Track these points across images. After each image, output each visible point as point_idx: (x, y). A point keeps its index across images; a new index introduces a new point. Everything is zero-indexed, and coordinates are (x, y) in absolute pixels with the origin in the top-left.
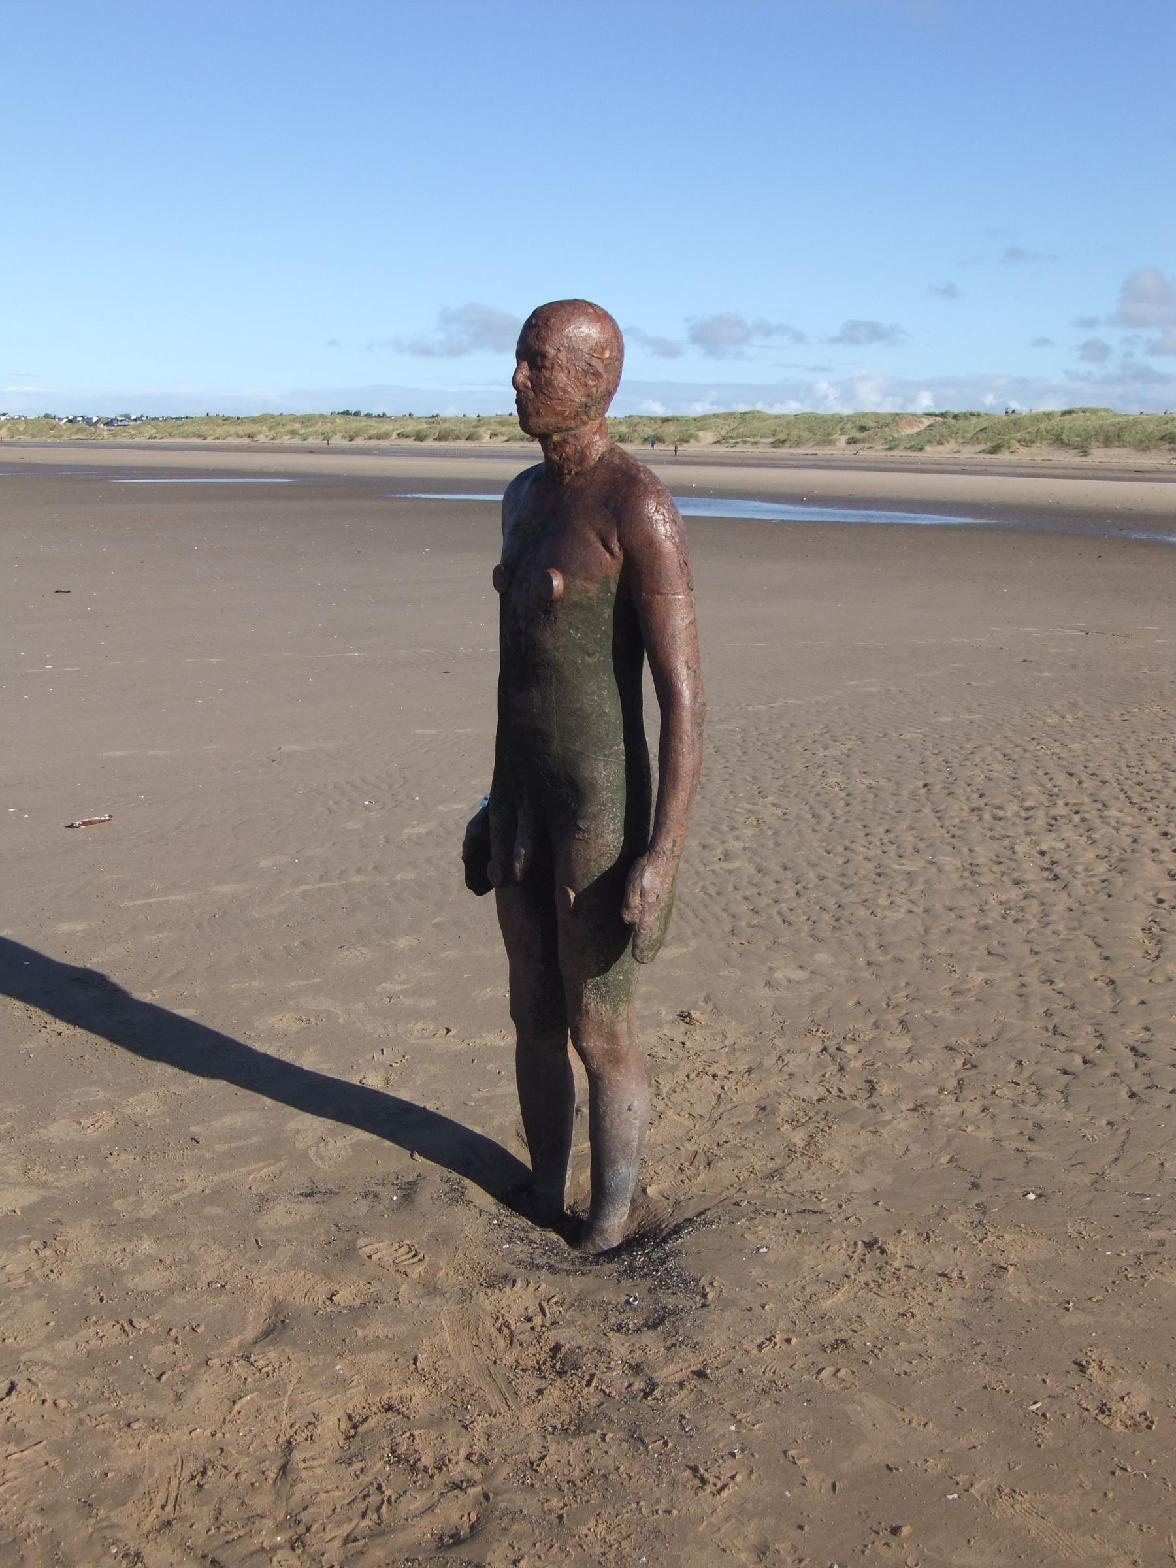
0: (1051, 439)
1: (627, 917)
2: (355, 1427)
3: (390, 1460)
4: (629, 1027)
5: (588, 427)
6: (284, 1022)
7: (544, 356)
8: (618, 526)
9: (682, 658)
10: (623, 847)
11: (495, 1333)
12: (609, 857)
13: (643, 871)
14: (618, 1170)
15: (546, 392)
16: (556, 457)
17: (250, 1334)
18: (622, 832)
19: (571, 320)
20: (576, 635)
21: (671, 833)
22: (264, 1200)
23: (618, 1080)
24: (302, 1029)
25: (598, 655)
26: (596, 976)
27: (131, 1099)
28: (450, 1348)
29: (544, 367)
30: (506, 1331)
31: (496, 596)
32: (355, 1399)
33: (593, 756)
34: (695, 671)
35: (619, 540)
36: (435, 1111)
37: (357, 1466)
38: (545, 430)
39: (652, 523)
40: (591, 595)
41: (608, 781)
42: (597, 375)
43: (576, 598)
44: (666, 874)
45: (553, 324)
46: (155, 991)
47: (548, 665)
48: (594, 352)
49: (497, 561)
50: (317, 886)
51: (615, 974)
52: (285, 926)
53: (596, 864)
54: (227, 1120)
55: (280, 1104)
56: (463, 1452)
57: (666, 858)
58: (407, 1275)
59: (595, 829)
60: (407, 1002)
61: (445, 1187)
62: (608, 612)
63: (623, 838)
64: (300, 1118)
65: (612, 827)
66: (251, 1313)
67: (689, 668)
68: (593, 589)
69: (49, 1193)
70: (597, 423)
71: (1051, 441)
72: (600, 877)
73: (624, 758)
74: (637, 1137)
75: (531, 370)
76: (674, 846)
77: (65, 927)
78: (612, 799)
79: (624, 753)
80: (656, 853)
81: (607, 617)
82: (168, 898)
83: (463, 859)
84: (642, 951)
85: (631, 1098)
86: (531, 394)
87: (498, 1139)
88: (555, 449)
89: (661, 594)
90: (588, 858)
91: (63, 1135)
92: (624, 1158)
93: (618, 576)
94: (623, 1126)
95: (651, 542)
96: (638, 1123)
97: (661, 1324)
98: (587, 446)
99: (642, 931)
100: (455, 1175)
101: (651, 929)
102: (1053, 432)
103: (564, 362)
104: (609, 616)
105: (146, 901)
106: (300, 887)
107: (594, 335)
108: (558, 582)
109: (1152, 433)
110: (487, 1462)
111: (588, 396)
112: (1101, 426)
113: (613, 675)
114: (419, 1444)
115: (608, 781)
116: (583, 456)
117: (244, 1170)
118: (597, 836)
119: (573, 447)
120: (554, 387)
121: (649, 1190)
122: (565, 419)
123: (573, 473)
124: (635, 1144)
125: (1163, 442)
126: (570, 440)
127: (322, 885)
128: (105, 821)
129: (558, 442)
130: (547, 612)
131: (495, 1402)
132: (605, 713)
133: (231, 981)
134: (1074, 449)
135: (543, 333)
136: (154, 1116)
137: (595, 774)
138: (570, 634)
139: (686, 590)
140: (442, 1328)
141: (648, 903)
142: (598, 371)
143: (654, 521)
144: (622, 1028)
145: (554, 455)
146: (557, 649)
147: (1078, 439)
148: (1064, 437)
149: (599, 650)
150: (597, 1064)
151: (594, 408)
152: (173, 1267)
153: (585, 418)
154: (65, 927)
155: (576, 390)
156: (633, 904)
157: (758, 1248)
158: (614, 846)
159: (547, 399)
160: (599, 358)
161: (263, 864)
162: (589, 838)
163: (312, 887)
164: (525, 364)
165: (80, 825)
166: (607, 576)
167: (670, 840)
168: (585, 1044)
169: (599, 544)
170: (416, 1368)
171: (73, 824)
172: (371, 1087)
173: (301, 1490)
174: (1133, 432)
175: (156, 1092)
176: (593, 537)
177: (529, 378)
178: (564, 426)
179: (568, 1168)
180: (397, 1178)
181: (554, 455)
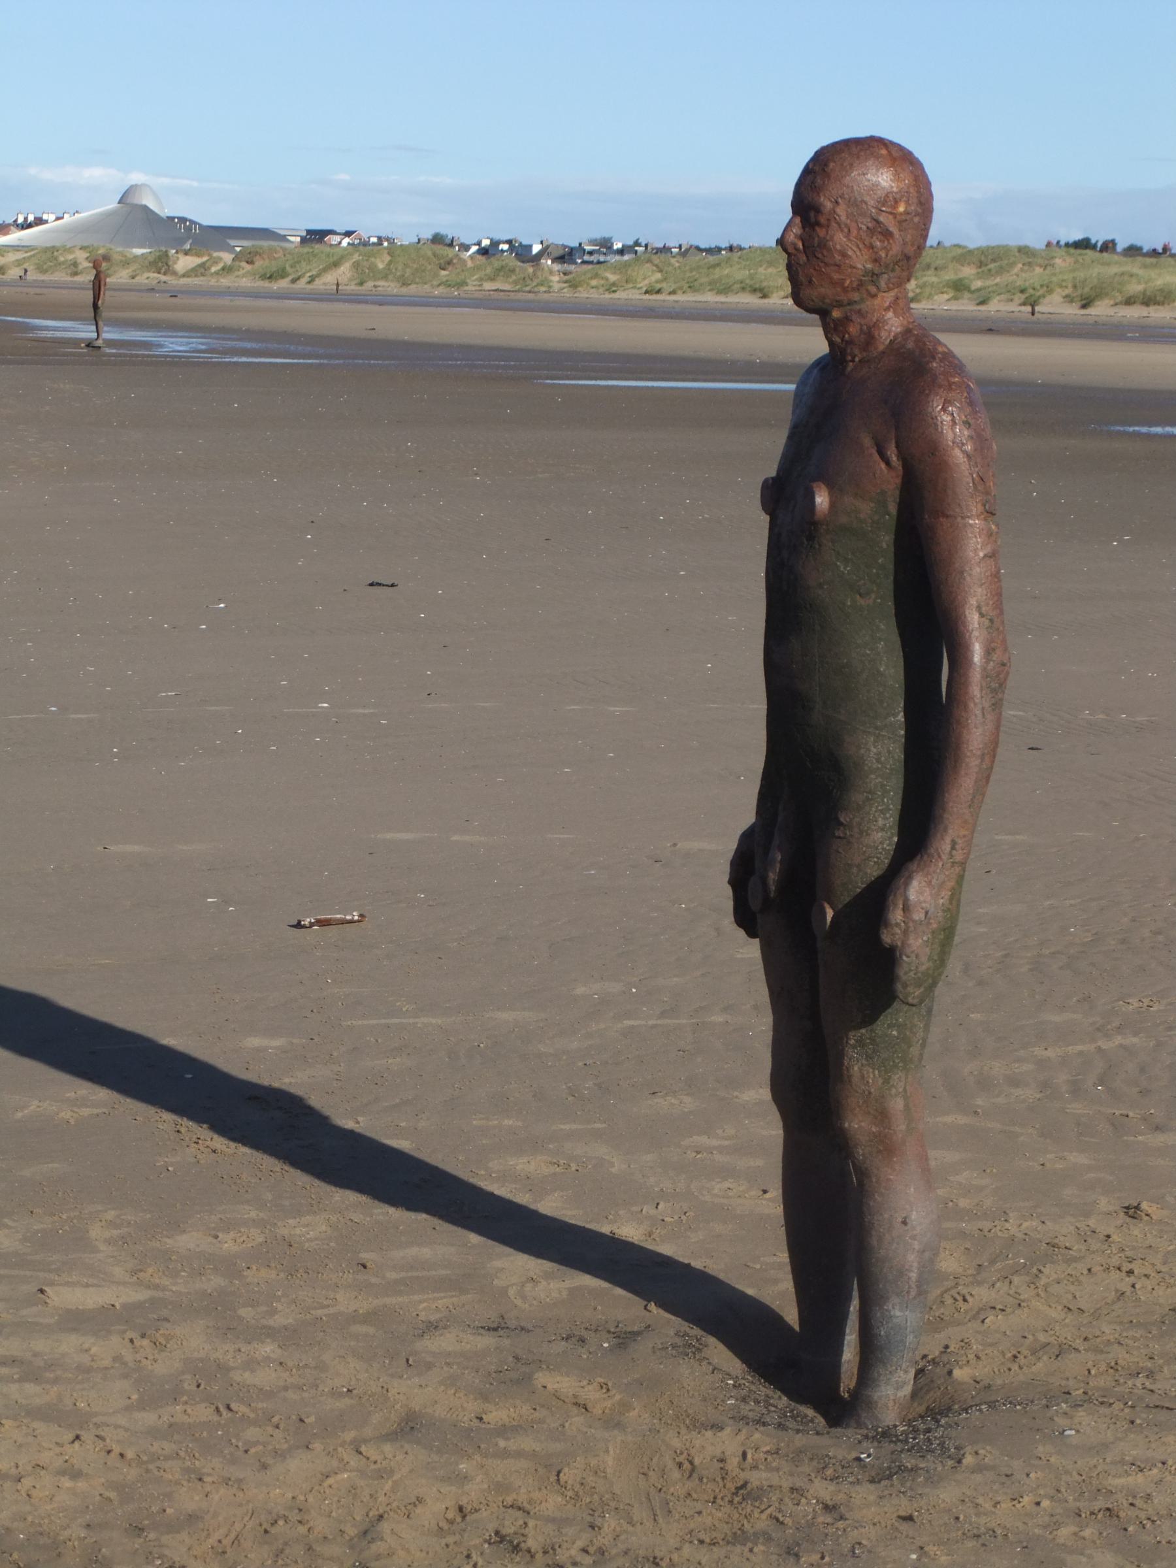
1: (886, 938)
2: (464, 1517)
3: (490, 1539)
4: (906, 1106)
5: (877, 301)
6: (527, 1164)
7: (818, 210)
8: (896, 429)
9: (973, 601)
10: (895, 850)
11: (670, 1464)
12: (875, 862)
13: (910, 878)
14: (889, 1311)
15: (820, 256)
16: (837, 340)
17: (368, 1432)
18: (895, 830)
19: (855, 165)
20: (845, 568)
21: (950, 831)
22: (432, 1327)
23: (890, 1180)
24: (555, 1174)
25: (873, 596)
26: (861, 1028)
27: (291, 1221)
28: (608, 1470)
29: (818, 224)
30: (687, 1465)
31: (767, 518)
32: (473, 1492)
33: (861, 728)
34: (991, 621)
35: (897, 447)
36: (702, 1268)
37: (450, 1539)
38: (821, 304)
39: (936, 425)
40: (862, 516)
41: (878, 761)
42: (887, 234)
43: (844, 519)
44: (942, 885)
45: (831, 170)
46: (360, 1119)
47: (810, 605)
48: (883, 205)
49: (773, 473)
50: (651, 1023)
51: (887, 1026)
52: (580, 1064)
53: (860, 870)
54: (413, 1251)
55: (490, 1242)
56: (580, 1544)
57: (940, 864)
58: (586, 1409)
59: (860, 824)
60: (718, 1157)
61: (679, 1341)
62: (886, 540)
63: (896, 839)
64: (512, 1258)
65: (881, 822)
66: (376, 1418)
67: (982, 615)
68: (866, 509)
69: (160, 1294)
70: (889, 297)
72: (865, 889)
73: (903, 732)
74: (915, 1264)
75: (803, 228)
76: (953, 848)
77: (254, 1042)
78: (883, 786)
79: (903, 726)
80: (928, 857)
81: (884, 545)
82: (417, 1020)
83: (730, 882)
84: (905, 986)
85: (907, 1207)
86: (803, 259)
87: (775, 1305)
88: (835, 329)
89: (947, 516)
90: (849, 862)
91: (192, 1246)
92: (898, 1295)
93: (897, 492)
94: (895, 1245)
95: (934, 450)
96: (916, 1245)
97: (888, 1479)
98: (875, 325)
99: (904, 958)
100: (696, 1331)
101: (917, 956)
103: (843, 218)
104: (887, 545)
105: (383, 1021)
106: (625, 1022)
107: (884, 184)
108: (822, 500)
110: (603, 1554)
111: (876, 260)
113: (893, 621)
114: (530, 1531)
115: (878, 761)
116: (870, 337)
117: (416, 1298)
118: (861, 832)
119: (858, 327)
120: (829, 250)
121: (957, 1373)
122: (845, 290)
123: (857, 359)
124: (914, 1275)
126: (854, 317)
127: (659, 1022)
128: (352, 922)
129: (838, 319)
130: (811, 538)
131: (639, 1513)
132: (878, 671)
133: (474, 1117)
135: (819, 181)
136: (316, 1239)
137: (862, 751)
138: (838, 567)
139: (982, 513)
140: (607, 1451)
141: (914, 921)
142: (887, 230)
143: (939, 423)
144: (897, 1105)
145: (834, 336)
146: (820, 586)
149: (875, 589)
150: (863, 1155)
151: (886, 276)
152: (294, 1370)
153: (873, 289)
154: (254, 1042)
155: (858, 253)
156: (893, 922)
157: (1064, 1431)
158: (883, 849)
159: (820, 264)
160: (891, 213)
161: (580, 990)
162: (851, 836)
163: (643, 1022)
164: (798, 220)
165: (312, 925)
166: (883, 493)
167: (948, 840)
168: (846, 1125)
169: (874, 451)
170: (558, 1480)
171: (299, 922)
172: (624, 1238)
173: (378, 1547)
175: (327, 1217)
176: (867, 441)
177: (801, 238)
178: (844, 298)
179: (848, 1331)
180: (617, 1326)
181: (834, 336)
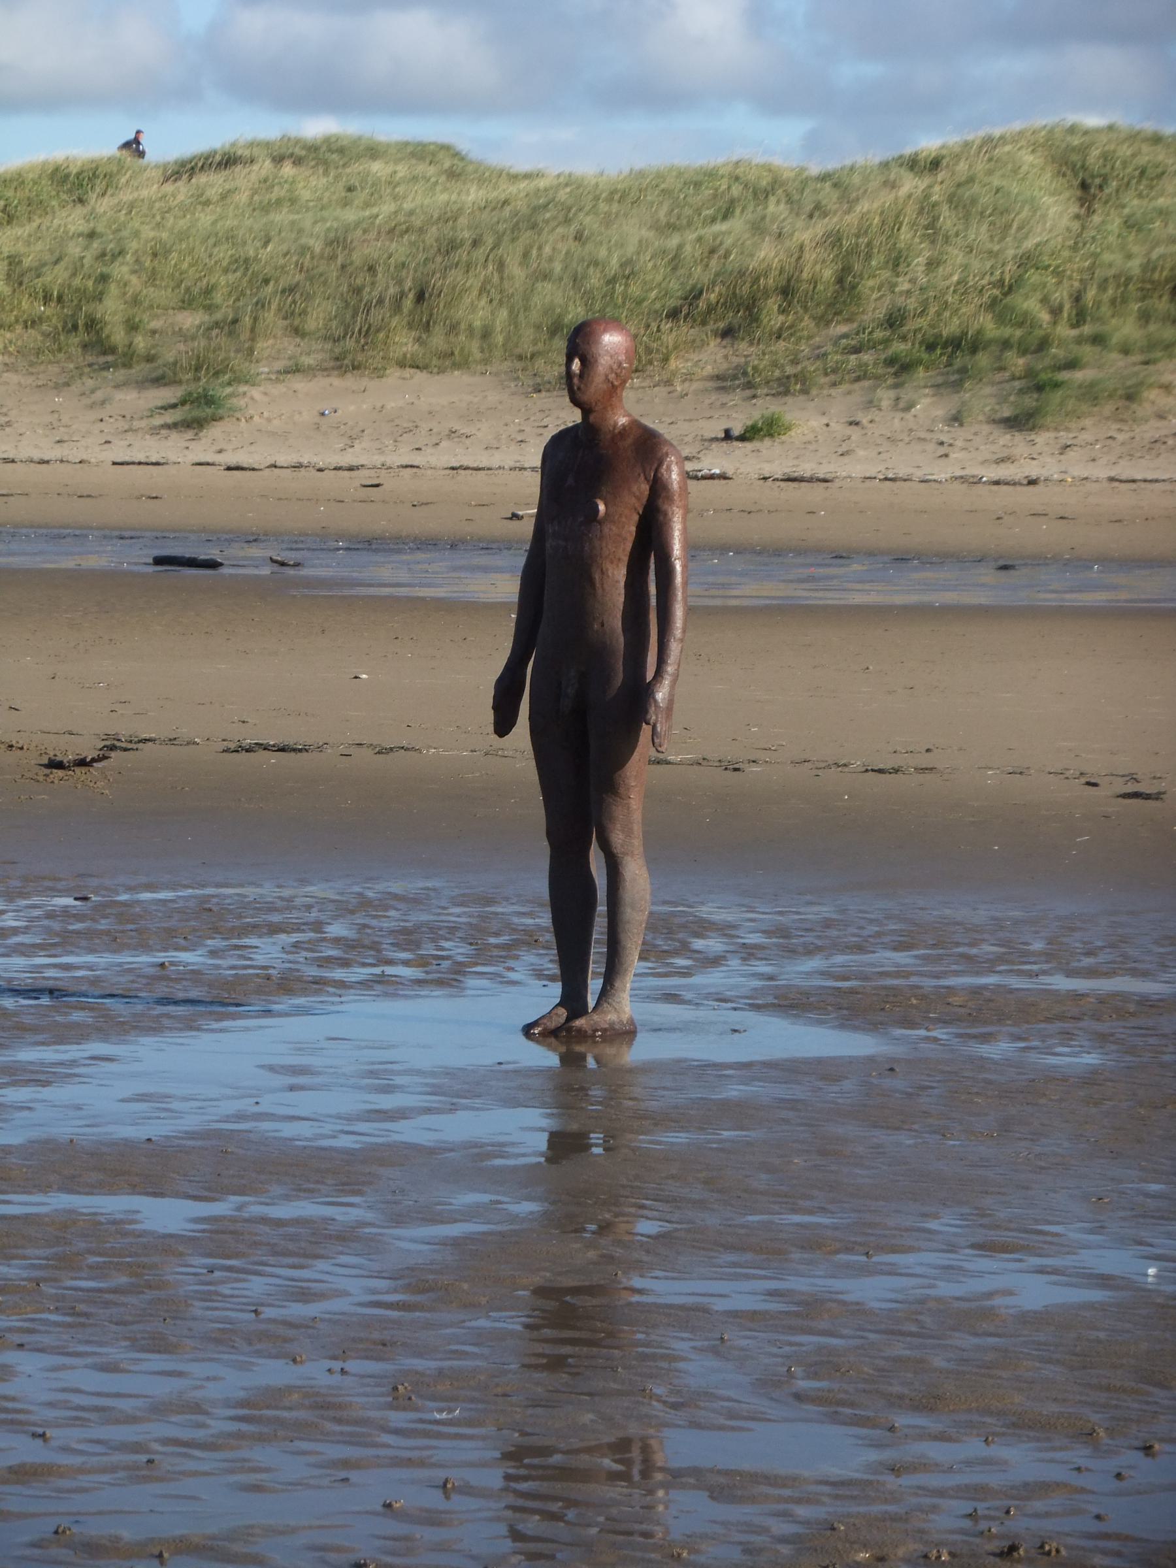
0: (33, 323)
71: (33, 337)
102: (56, 277)
109: (628, 270)
112: (338, 242)
125: (685, 331)
134: (143, 384)
147: (190, 320)
148: (112, 309)
174: (516, 270)
